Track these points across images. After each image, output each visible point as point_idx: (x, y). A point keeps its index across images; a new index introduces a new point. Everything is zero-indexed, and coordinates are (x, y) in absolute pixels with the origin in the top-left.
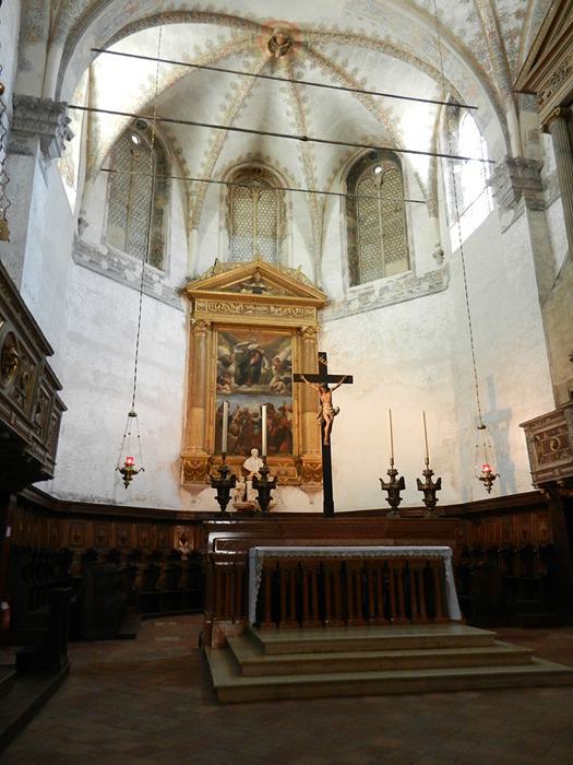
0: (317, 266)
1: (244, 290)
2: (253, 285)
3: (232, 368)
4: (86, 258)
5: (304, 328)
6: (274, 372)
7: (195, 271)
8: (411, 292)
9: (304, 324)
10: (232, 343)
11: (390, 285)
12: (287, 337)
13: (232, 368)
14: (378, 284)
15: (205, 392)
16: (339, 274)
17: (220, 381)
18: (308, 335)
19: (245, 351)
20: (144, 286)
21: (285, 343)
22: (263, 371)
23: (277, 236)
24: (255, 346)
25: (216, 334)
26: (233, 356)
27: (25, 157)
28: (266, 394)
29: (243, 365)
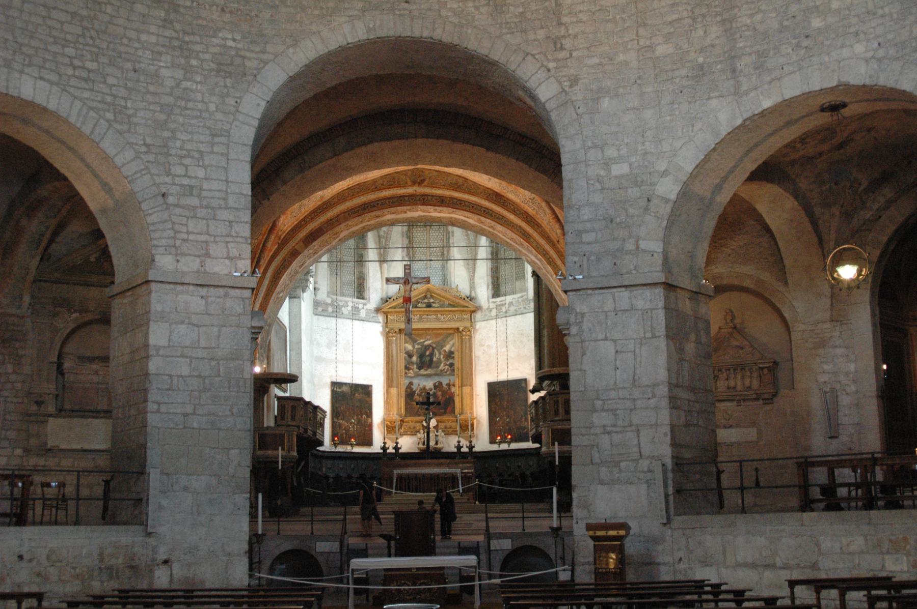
0: (472, 279)
2: (426, 301)
3: (414, 359)
4: (320, 309)
5: (461, 329)
6: (442, 359)
7: (387, 293)
8: (525, 308)
10: (414, 341)
11: (514, 301)
12: (451, 334)
13: (414, 359)
14: (509, 299)
15: (397, 376)
17: (407, 368)
18: (464, 333)
19: (422, 346)
20: (354, 315)
21: (449, 339)
22: (435, 359)
23: (445, 259)
24: (430, 342)
25: (403, 336)
28: (436, 375)
29: (421, 356)
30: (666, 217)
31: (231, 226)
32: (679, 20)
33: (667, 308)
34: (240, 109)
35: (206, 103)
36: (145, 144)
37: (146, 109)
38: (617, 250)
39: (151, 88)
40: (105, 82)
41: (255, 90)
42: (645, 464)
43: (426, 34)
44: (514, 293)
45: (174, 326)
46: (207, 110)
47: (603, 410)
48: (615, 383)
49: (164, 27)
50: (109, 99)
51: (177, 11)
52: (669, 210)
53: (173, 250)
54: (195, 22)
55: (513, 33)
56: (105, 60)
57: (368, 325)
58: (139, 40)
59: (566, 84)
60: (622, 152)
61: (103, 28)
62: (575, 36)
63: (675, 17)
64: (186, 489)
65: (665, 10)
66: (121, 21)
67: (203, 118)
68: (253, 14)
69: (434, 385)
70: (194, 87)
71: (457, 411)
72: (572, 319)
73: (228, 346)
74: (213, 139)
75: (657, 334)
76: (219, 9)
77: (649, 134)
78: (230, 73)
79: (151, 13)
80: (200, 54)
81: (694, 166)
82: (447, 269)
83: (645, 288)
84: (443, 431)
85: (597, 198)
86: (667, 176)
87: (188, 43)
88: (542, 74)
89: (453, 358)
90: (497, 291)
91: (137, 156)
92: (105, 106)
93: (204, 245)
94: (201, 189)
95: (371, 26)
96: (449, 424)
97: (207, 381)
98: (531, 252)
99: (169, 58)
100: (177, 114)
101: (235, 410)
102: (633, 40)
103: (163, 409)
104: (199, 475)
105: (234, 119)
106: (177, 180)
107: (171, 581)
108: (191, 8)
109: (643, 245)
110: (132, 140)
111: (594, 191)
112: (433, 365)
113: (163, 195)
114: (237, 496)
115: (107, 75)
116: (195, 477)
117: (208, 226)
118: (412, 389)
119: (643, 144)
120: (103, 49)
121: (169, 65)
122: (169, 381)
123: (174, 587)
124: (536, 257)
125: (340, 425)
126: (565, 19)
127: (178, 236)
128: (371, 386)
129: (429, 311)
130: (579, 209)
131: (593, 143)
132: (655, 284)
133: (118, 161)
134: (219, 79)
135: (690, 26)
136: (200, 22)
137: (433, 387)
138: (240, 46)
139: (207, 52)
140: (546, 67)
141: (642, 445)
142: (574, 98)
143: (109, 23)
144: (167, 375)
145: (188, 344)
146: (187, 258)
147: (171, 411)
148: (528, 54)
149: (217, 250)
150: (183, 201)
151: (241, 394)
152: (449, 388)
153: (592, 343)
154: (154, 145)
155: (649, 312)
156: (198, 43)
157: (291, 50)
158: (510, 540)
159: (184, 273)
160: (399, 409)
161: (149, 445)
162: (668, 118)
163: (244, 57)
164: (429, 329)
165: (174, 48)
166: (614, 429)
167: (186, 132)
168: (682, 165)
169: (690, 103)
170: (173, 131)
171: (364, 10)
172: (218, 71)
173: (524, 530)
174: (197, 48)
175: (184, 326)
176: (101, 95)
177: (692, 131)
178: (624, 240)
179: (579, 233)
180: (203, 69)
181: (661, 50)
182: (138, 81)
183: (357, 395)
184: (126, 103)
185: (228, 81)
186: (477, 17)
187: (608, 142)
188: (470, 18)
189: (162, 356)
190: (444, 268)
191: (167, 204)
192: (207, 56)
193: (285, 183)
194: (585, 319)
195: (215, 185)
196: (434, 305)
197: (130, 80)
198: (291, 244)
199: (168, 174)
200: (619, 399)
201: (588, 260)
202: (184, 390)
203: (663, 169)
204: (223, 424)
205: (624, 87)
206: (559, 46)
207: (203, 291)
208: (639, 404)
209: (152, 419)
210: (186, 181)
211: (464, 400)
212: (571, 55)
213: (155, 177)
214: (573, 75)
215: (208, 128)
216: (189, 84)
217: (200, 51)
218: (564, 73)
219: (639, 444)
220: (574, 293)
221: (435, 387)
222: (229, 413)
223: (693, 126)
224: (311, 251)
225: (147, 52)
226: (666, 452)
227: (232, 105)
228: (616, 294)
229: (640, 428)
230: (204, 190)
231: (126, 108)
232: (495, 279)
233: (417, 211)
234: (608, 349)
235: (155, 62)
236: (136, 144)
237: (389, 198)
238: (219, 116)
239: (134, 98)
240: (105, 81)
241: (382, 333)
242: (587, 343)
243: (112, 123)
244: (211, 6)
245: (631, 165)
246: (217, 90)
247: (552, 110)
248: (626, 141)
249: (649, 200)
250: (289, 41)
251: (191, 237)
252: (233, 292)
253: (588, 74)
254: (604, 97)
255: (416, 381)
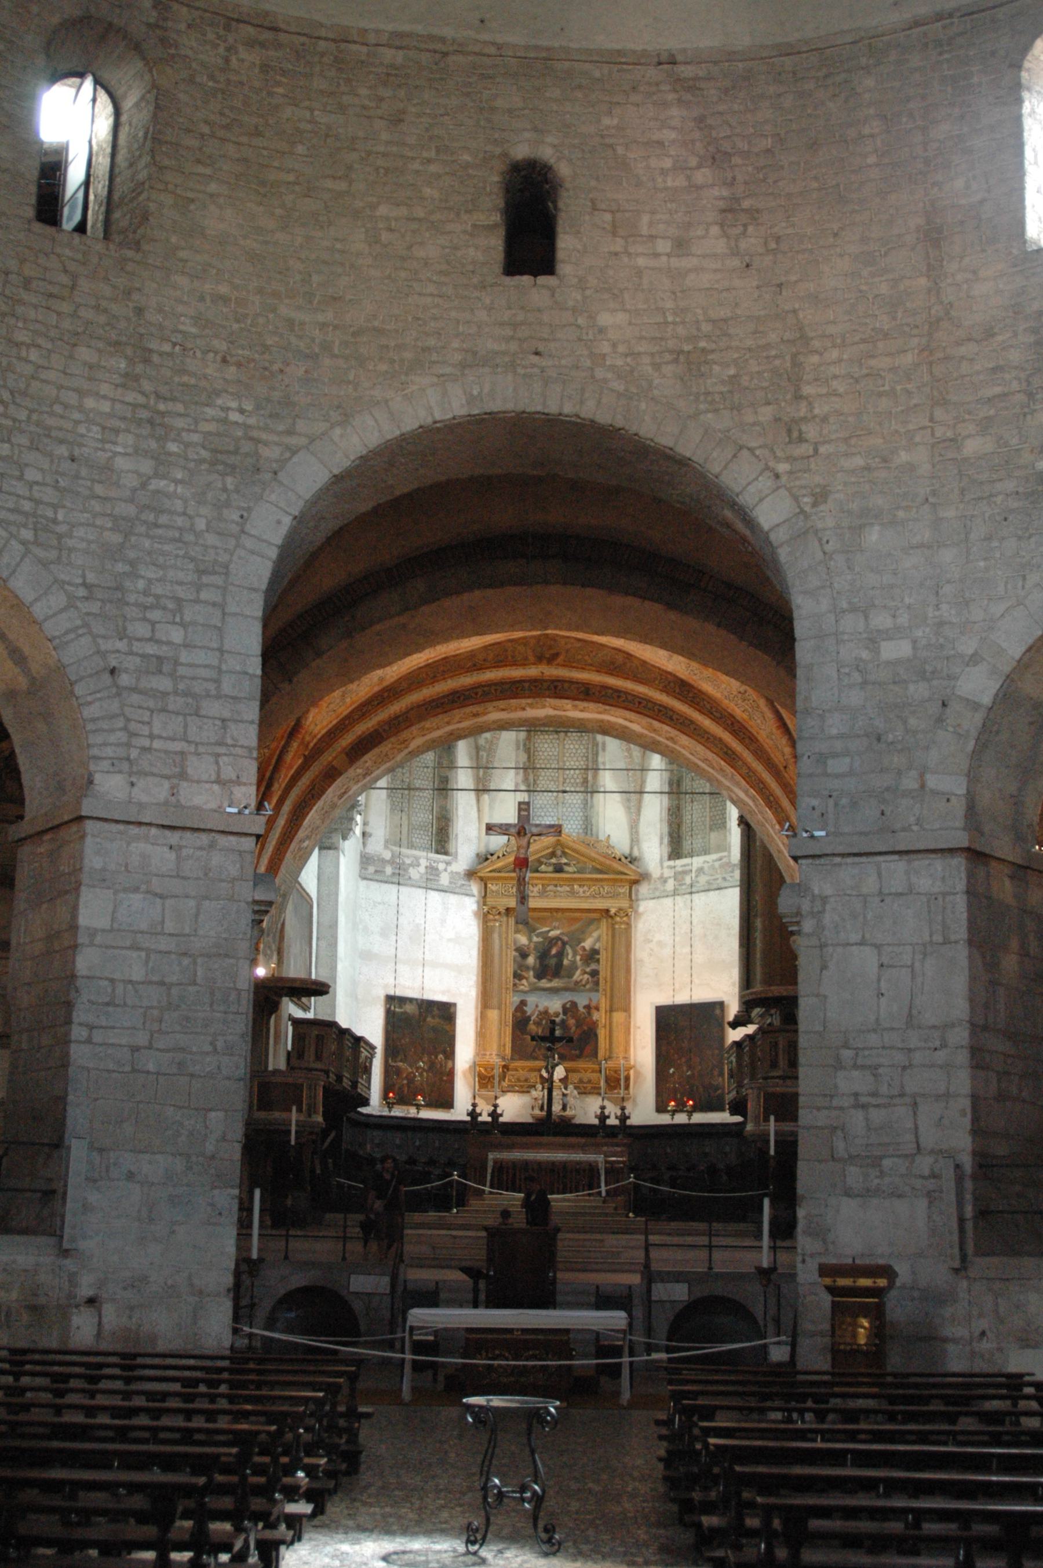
1: (543, 868)
2: (554, 861)
3: (531, 960)
4: (371, 869)
5: (613, 911)
6: (579, 963)
8: (724, 879)
9: (613, 905)
10: (531, 930)
11: (706, 866)
13: (531, 960)
14: (697, 862)
16: (657, 844)
17: (517, 976)
19: (545, 938)
20: (430, 882)
21: (592, 927)
22: (566, 962)
23: (590, 789)
26: (532, 945)
27: (331, 852)
28: (567, 989)
29: (543, 956)
30: (974, 733)
31: (224, 728)
32: (1004, 395)
33: (970, 892)
34: (248, 527)
35: (190, 517)
36: (84, 584)
37: (88, 525)
38: (888, 789)
39: (99, 490)
40: (21, 478)
41: (273, 497)
42: (925, 1164)
43: (568, 409)
44: (706, 852)
45: (122, 895)
46: (192, 529)
47: (856, 1067)
48: (877, 1019)
49: (124, 386)
50: (27, 506)
51: (147, 361)
52: (980, 725)
53: (125, 766)
54: (176, 379)
55: (716, 411)
56: (24, 440)
57: (453, 899)
58: (80, 408)
59: (806, 500)
60: (899, 621)
61: (22, 386)
62: (825, 419)
63: (998, 390)
64: (130, 1176)
65: (982, 377)
66: (51, 375)
67: (185, 543)
68: (275, 367)
69: (564, 1007)
70: (172, 488)
71: (601, 1053)
72: (806, 906)
73: (212, 933)
74: (199, 579)
75: (953, 938)
76: (219, 358)
77: (947, 589)
78: (233, 467)
79: (103, 363)
80: (184, 434)
81: (1024, 649)
82: (592, 807)
83: (933, 856)
84: (576, 1088)
85: (855, 698)
86: (976, 664)
87: (163, 414)
88: (765, 483)
89: (598, 961)
90: (676, 848)
91: (71, 605)
92: (20, 519)
93: (178, 759)
94: (177, 663)
95: (475, 393)
96: (586, 1076)
97: (174, 991)
98: (738, 784)
99: (130, 439)
100: (140, 535)
101: (220, 1044)
102: (924, 428)
103: (98, 1037)
104: (154, 1153)
105: (237, 546)
106: (137, 647)
107: (99, 1335)
108: (170, 355)
109: (932, 781)
110: (62, 577)
111: (851, 686)
112: (563, 973)
113: (113, 671)
114: (216, 1192)
115: (26, 465)
116: (147, 1156)
117: (186, 726)
118: (525, 1012)
119: (937, 607)
120: (20, 422)
121: (130, 450)
122: (109, 990)
123: (104, 1346)
124: (746, 792)
125: (398, 1072)
126: (807, 390)
127: (135, 741)
128: (455, 1005)
129: (559, 879)
130: (822, 717)
131: (850, 603)
132: (951, 851)
133: (39, 610)
134: (216, 476)
135: (1022, 407)
136: (185, 379)
137: (560, 1010)
138: (252, 421)
139: (196, 431)
140: (772, 470)
141: (921, 1129)
142: (820, 525)
143: (33, 377)
144: (107, 979)
145: (144, 926)
146: (150, 779)
147: (111, 1041)
148: (741, 448)
149: (200, 767)
150: (144, 684)
151: (231, 1017)
152: (589, 1013)
153: (840, 950)
154: (99, 586)
155: (940, 899)
156: (180, 415)
157: (338, 431)
158: (686, 1285)
159: (141, 805)
160: (501, 1046)
161: (71, 1098)
162: (982, 564)
163: (257, 441)
164: (557, 910)
165: (139, 422)
166: (873, 1101)
167: (154, 564)
168: (1004, 645)
169: (1020, 538)
170: (132, 564)
171: (463, 366)
172: (213, 463)
173: (710, 1268)
174: (180, 423)
175: (138, 897)
176: (15, 499)
177: (1023, 587)
178: (899, 773)
179: (822, 759)
180: (186, 459)
181: (972, 447)
182: (77, 477)
183: (429, 1019)
184: (56, 513)
185: (229, 480)
186: (656, 382)
187: (877, 602)
188: (644, 383)
189: (100, 946)
190: (587, 807)
191: (118, 687)
192: (195, 438)
193: (319, 654)
194: (828, 907)
195: (200, 657)
196: (566, 868)
197: (63, 474)
198: (327, 758)
199: (122, 635)
200: (883, 1047)
201: (836, 804)
202: (134, 1007)
203: (970, 652)
204: (197, 1067)
205: (907, 508)
206: (795, 434)
207: (174, 837)
208: (918, 1057)
209: (79, 1053)
210: (150, 649)
211: (615, 1034)
212: (816, 451)
213: (100, 641)
214: (818, 485)
215: (192, 559)
216: (163, 483)
217: (183, 429)
218: (803, 482)
219: (916, 1128)
220: (810, 861)
221: (565, 1010)
222: (210, 1049)
223: (1024, 578)
224: (359, 771)
225: (95, 428)
226: (962, 1142)
227: (233, 521)
228: (883, 865)
229: (918, 1099)
230: (182, 664)
231: (55, 521)
232: (675, 826)
233: (544, 707)
234: (867, 959)
235: (107, 446)
236: (69, 584)
237: (496, 684)
238: (211, 539)
239: (68, 505)
240: (22, 475)
241: (476, 914)
242: (830, 949)
243: (30, 546)
244: (205, 352)
245: (914, 642)
246: (210, 495)
247: (781, 545)
248: (907, 600)
249: (944, 705)
250: (335, 416)
251: (157, 744)
252: (224, 841)
253: (845, 484)
254: (872, 524)
255: (532, 999)
